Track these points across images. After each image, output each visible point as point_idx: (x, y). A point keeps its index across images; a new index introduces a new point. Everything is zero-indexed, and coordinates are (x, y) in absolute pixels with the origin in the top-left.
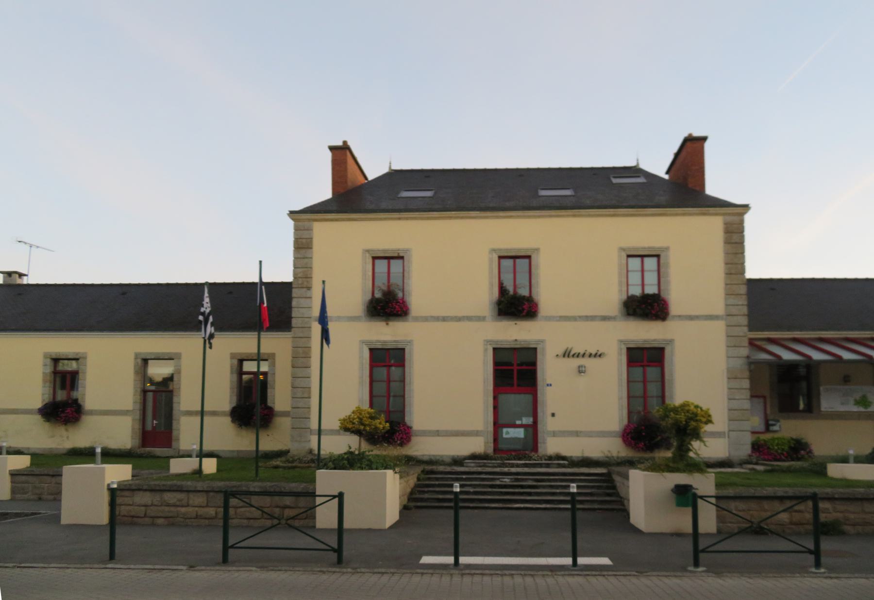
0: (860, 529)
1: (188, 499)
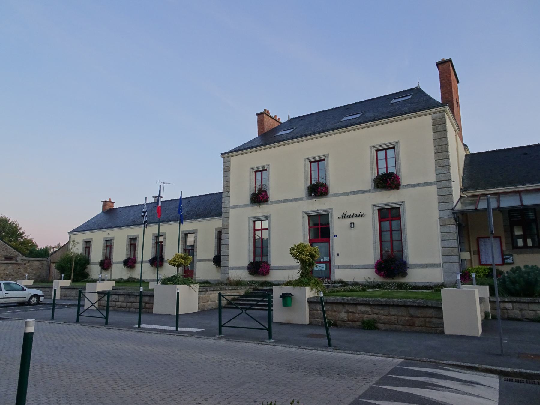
0: (388, 326)
1: (119, 298)
